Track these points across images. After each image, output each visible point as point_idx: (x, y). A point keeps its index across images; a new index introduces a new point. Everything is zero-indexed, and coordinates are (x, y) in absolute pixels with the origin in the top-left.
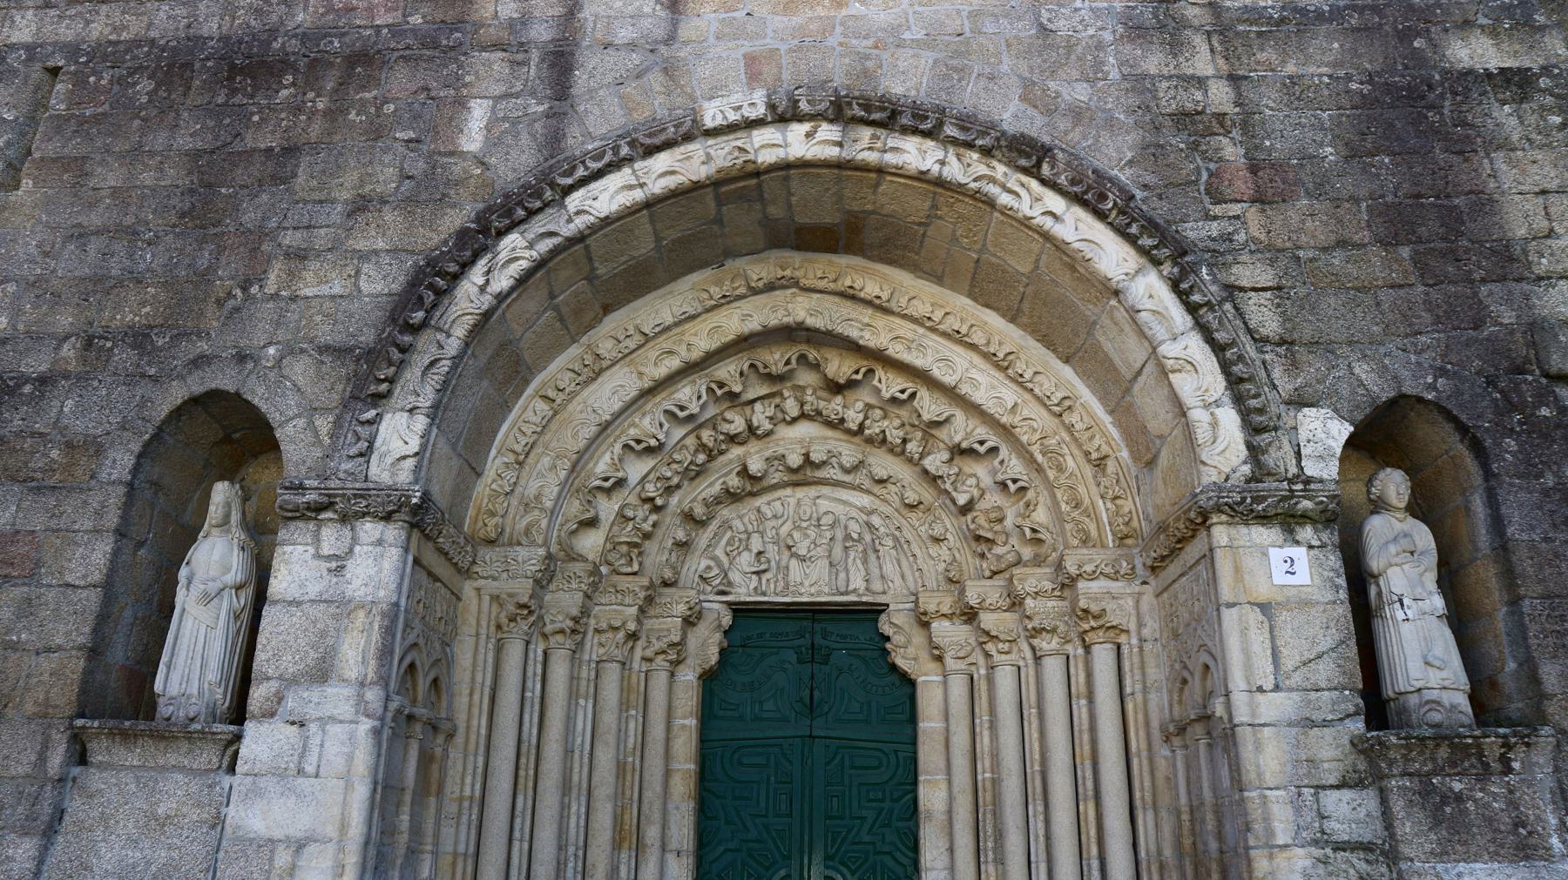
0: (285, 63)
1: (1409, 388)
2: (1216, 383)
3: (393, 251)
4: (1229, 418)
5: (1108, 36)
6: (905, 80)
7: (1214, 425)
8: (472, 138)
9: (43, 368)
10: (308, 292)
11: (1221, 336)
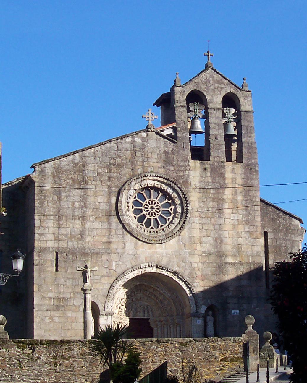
0: (88, 254)
1: (213, 304)
2: (194, 302)
3: (107, 283)
4: (195, 306)
5: (187, 256)
6: (164, 263)
7: (193, 306)
8: (114, 268)
9: (69, 297)
10: (98, 288)
11: (195, 297)
